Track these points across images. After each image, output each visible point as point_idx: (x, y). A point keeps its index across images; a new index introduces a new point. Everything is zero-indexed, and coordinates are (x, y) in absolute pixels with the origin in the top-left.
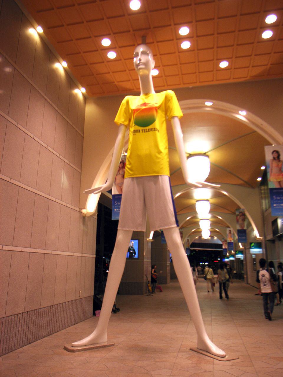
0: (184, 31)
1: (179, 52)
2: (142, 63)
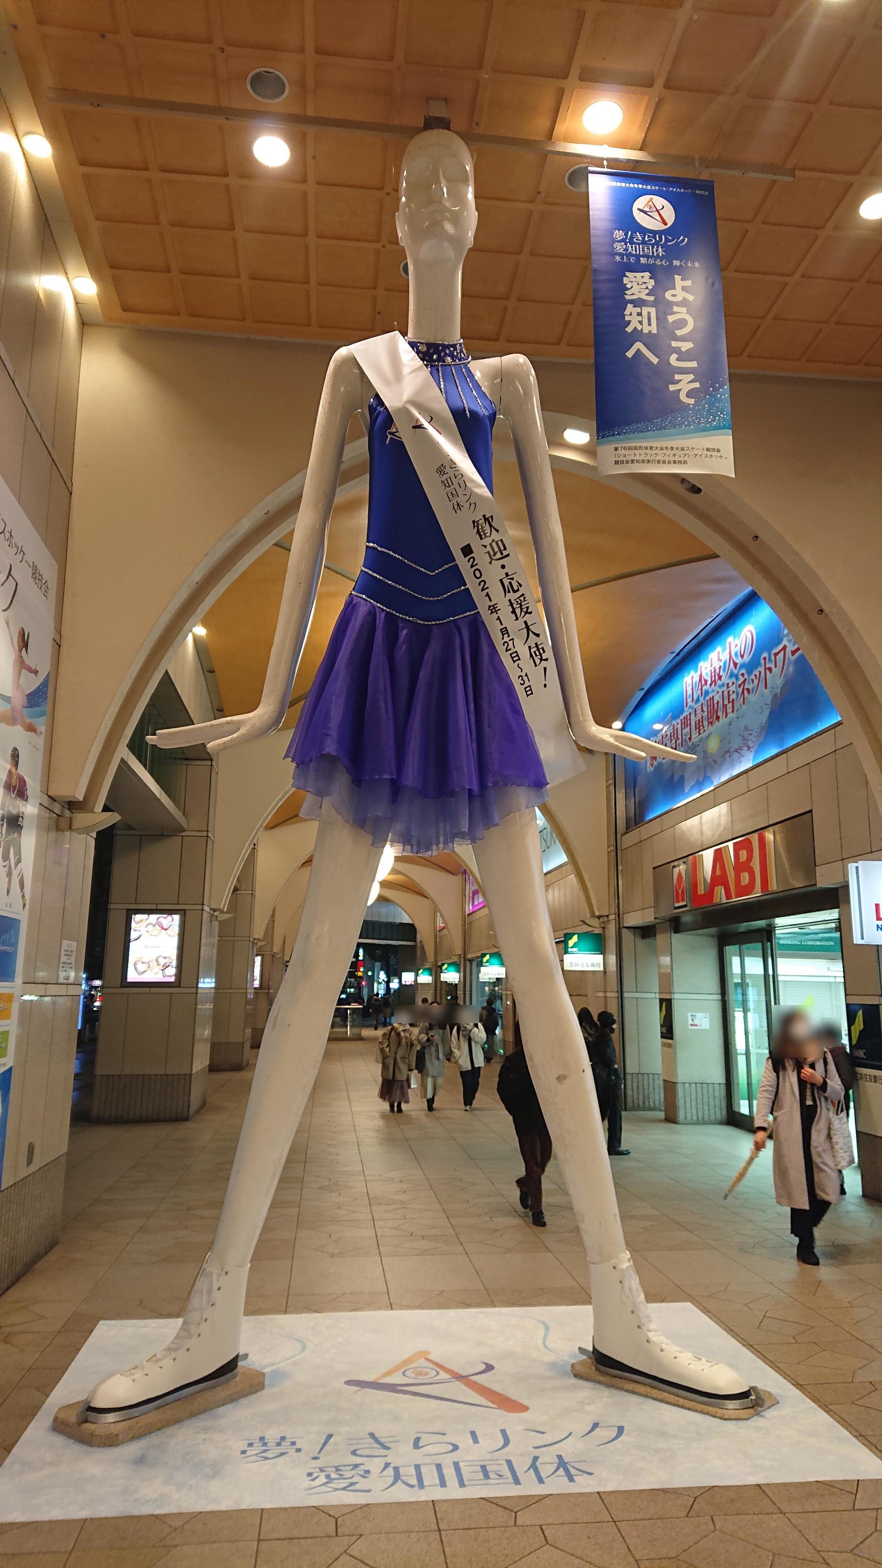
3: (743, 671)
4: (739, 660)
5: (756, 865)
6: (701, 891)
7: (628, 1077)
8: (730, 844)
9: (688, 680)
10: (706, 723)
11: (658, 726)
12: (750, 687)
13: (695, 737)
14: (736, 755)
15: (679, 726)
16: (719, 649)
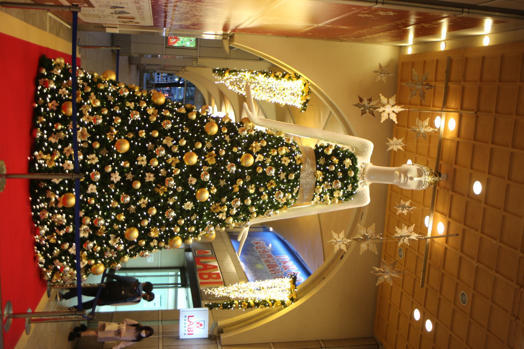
0: (441, 229)
6: (202, 260)
8: (219, 271)
9: (286, 257)
10: (268, 263)
11: (270, 245)
13: (263, 260)
16: (297, 269)
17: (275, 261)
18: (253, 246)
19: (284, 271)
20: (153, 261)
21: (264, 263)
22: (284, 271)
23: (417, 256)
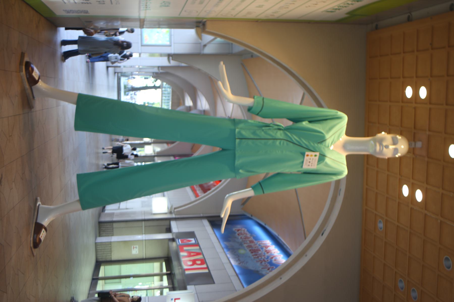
0: (419, 196)
1: (399, 179)
2: (383, 149)
3: (269, 261)
4: (273, 259)
5: (195, 266)
6: (185, 248)
7: (111, 224)
9: (268, 242)
10: (250, 248)
12: (263, 263)
13: (245, 245)
14: (237, 259)
15: (250, 239)
17: (257, 245)
18: (235, 233)
19: (267, 255)
20: (138, 253)
21: (246, 248)
22: (267, 255)
23: (398, 226)
